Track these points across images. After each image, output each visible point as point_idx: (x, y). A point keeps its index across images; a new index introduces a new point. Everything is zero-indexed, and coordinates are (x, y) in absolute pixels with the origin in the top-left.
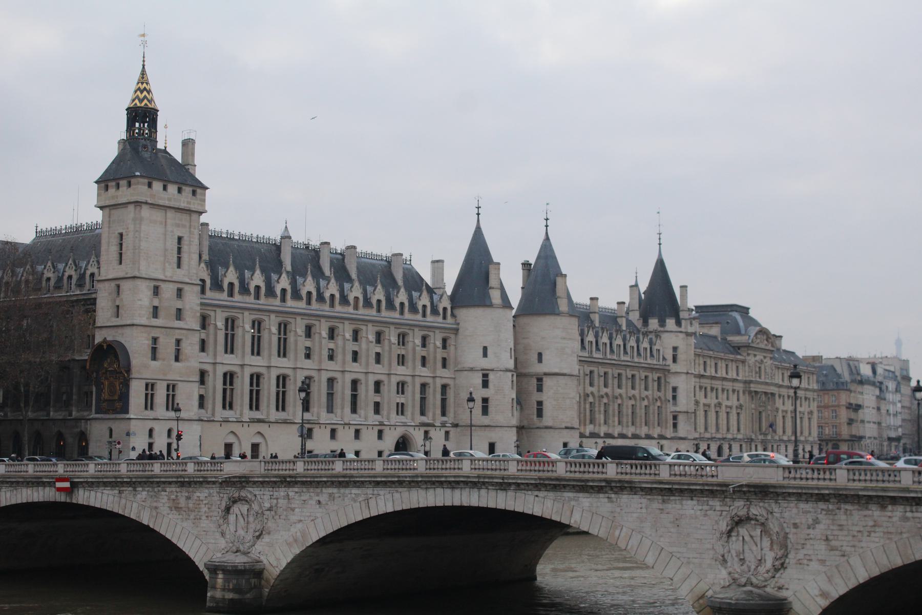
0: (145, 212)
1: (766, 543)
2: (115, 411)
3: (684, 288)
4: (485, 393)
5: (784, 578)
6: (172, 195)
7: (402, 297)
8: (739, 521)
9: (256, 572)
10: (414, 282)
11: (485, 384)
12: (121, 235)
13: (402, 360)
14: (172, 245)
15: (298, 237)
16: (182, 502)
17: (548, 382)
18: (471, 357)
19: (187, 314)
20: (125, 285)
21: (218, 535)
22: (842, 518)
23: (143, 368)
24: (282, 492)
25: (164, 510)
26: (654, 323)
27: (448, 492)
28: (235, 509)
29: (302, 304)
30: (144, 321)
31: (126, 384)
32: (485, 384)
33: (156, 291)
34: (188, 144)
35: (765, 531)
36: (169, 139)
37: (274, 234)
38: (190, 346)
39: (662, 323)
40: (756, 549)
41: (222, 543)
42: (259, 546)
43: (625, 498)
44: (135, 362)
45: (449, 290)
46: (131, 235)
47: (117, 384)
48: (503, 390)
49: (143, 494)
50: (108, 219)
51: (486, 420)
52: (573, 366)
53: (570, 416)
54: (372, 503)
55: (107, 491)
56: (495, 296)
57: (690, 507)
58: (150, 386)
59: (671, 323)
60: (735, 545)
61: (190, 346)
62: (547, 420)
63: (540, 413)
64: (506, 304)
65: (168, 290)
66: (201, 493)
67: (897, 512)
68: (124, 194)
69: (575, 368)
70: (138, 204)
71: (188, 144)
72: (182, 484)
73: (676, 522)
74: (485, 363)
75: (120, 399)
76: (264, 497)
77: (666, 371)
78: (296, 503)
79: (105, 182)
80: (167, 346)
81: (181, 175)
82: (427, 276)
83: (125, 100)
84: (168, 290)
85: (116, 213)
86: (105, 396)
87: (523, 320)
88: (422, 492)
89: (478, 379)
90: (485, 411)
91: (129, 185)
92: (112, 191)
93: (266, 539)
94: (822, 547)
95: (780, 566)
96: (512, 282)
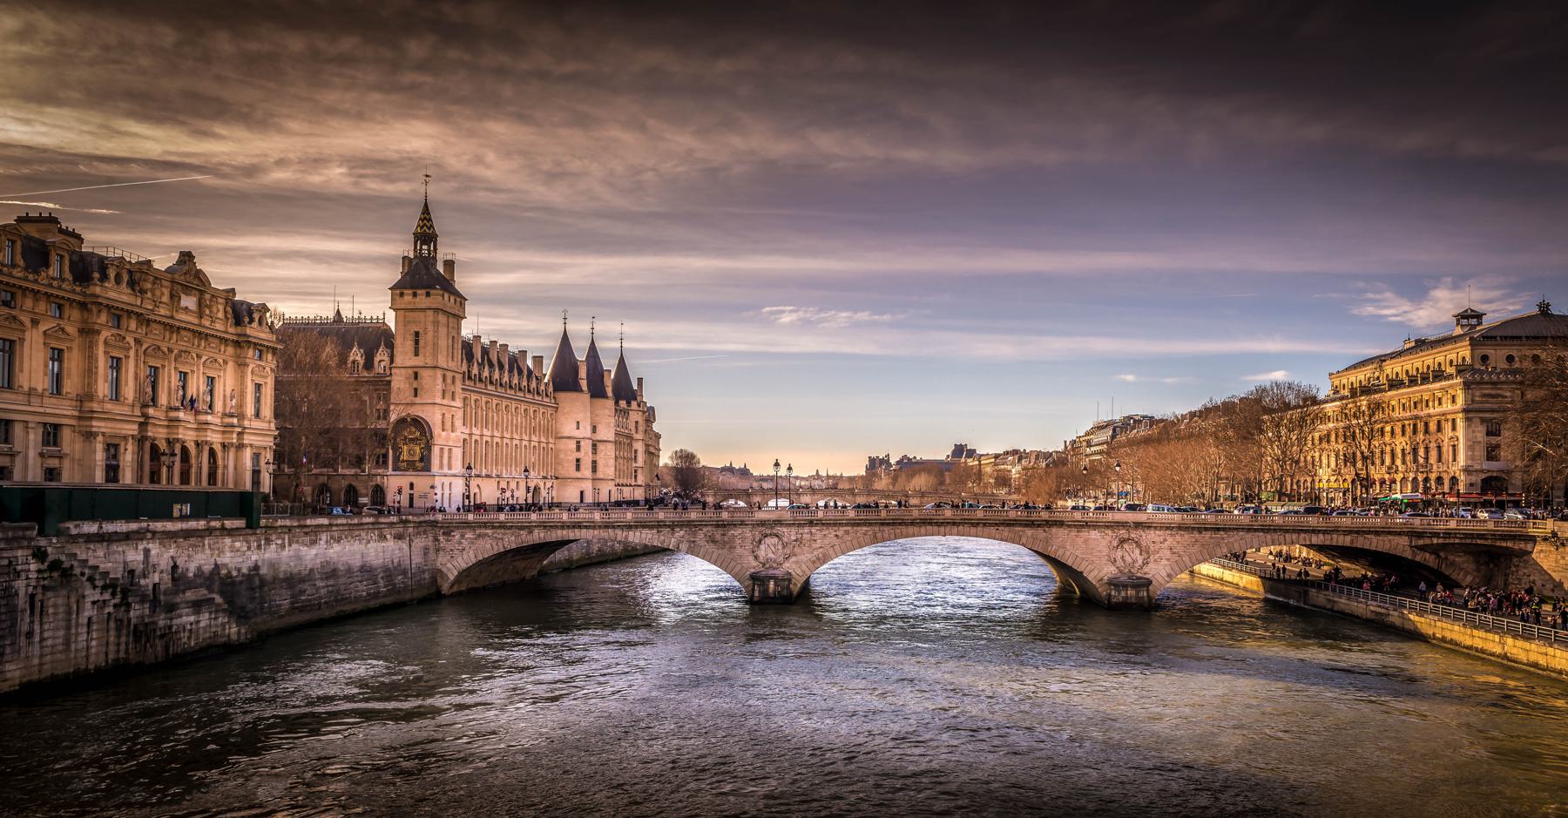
0: (442, 318)
1: (1137, 551)
2: (415, 469)
3: (640, 380)
4: (578, 455)
5: (1146, 569)
6: (448, 302)
7: (534, 385)
8: (1122, 541)
9: (788, 578)
11: (578, 449)
12: (417, 334)
16: (718, 537)
17: (600, 447)
18: (568, 428)
20: (424, 373)
21: (751, 558)
22: (1178, 538)
23: (440, 437)
24: (806, 530)
25: (702, 543)
26: (623, 403)
28: (769, 540)
30: (438, 401)
32: (578, 449)
33: (444, 377)
35: (1138, 545)
38: (458, 423)
39: (629, 403)
40: (1133, 555)
41: (754, 563)
42: (786, 565)
43: (1054, 530)
46: (430, 334)
47: (417, 449)
48: (586, 455)
49: (680, 533)
51: (578, 475)
52: (611, 437)
53: (611, 472)
55: (646, 531)
57: (1094, 534)
59: (634, 404)
60: (1119, 553)
61: (458, 423)
62: (600, 475)
63: (594, 469)
66: (737, 532)
67: (1208, 535)
68: (422, 300)
69: (612, 438)
70: (436, 310)
72: (718, 526)
73: (1086, 541)
74: (578, 434)
75: (421, 460)
76: (790, 534)
77: (631, 438)
78: (819, 535)
79: (398, 289)
83: (414, 224)
84: (449, 375)
86: (405, 456)
89: (573, 445)
90: (578, 468)
91: (428, 295)
92: (408, 298)
93: (793, 559)
94: (1168, 553)
95: (1146, 563)
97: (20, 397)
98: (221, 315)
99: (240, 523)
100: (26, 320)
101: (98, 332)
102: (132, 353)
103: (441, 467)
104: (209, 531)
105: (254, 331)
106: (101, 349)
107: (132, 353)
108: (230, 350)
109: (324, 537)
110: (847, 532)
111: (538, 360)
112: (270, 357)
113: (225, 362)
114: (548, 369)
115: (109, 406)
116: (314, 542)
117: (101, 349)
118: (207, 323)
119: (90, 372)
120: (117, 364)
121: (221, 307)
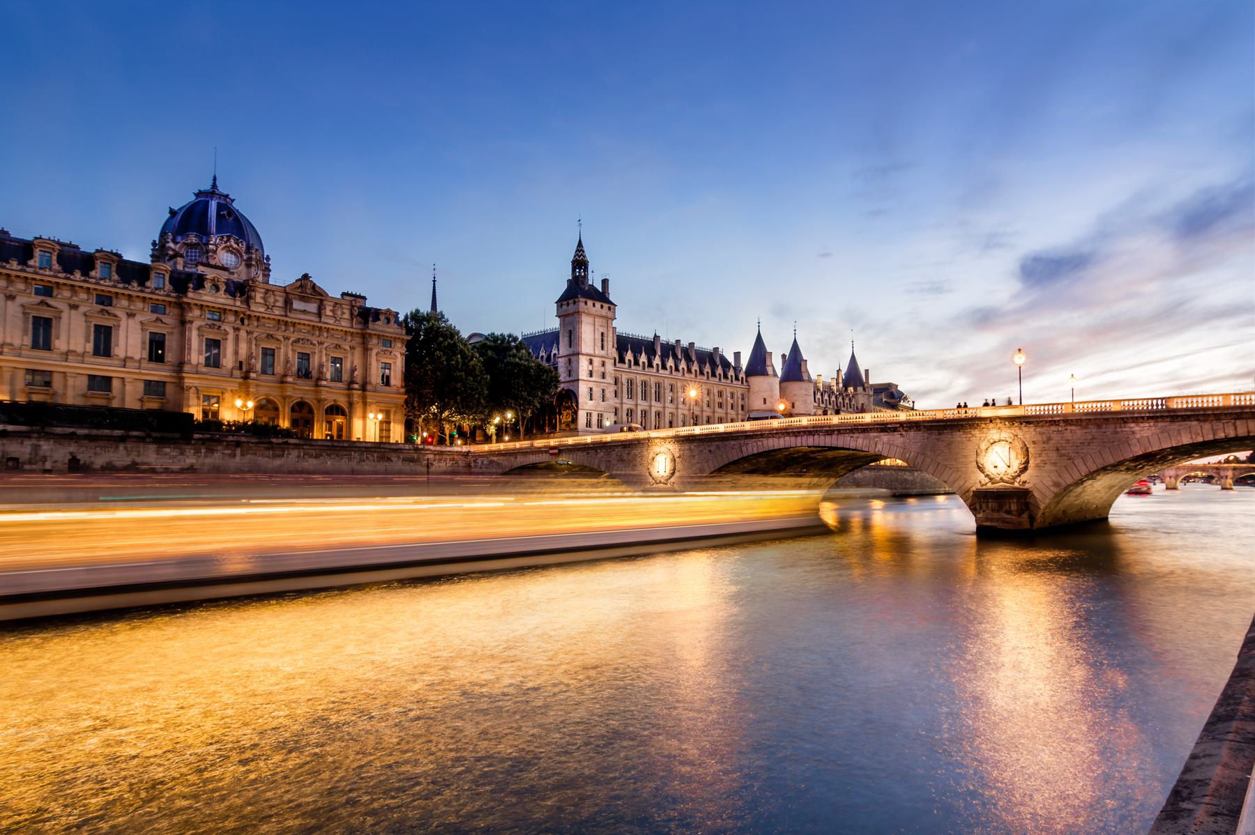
7: (720, 371)
10: (726, 364)
13: (720, 405)
14: (598, 337)
15: (663, 339)
16: (625, 457)
19: (607, 376)
20: (573, 358)
27: (793, 439)
29: (667, 372)
31: (576, 412)
33: (591, 362)
34: (605, 282)
36: (595, 280)
37: (650, 337)
44: (580, 400)
45: (744, 368)
50: (563, 324)
54: (744, 448)
56: (770, 370)
58: (589, 415)
61: (610, 393)
64: (775, 375)
65: (597, 361)
71: (605, 282)
79: (561, 302)
80: (597, 392)
81: (602, 297)
82: (731, 359)
84: (597, 361)
85: (568, 319)
87: (785, 384)
88: (776, 440)
96: (777, 365)
97: (117, 362)
98: (347, 316)
99: (177, 435)
100: (121, 314)
101: (191, 322)
102: (231, 337)
103: (589, 424)
104: (123, 439)
105: (379, 326)
106: (194, 334)
107: (231, 337)
108: (358, 340)
109: (295, 453)
110: (718, 447)
111: (737, 355)
112: (399, 345)
113: (352, 348)
114: (744, 363)
115: (205, 370)
116: (275, 456)
117: (194, 334)
118: (331, 321)
119: (183, 346)
120: (214, 344)
121: (347, 312)
